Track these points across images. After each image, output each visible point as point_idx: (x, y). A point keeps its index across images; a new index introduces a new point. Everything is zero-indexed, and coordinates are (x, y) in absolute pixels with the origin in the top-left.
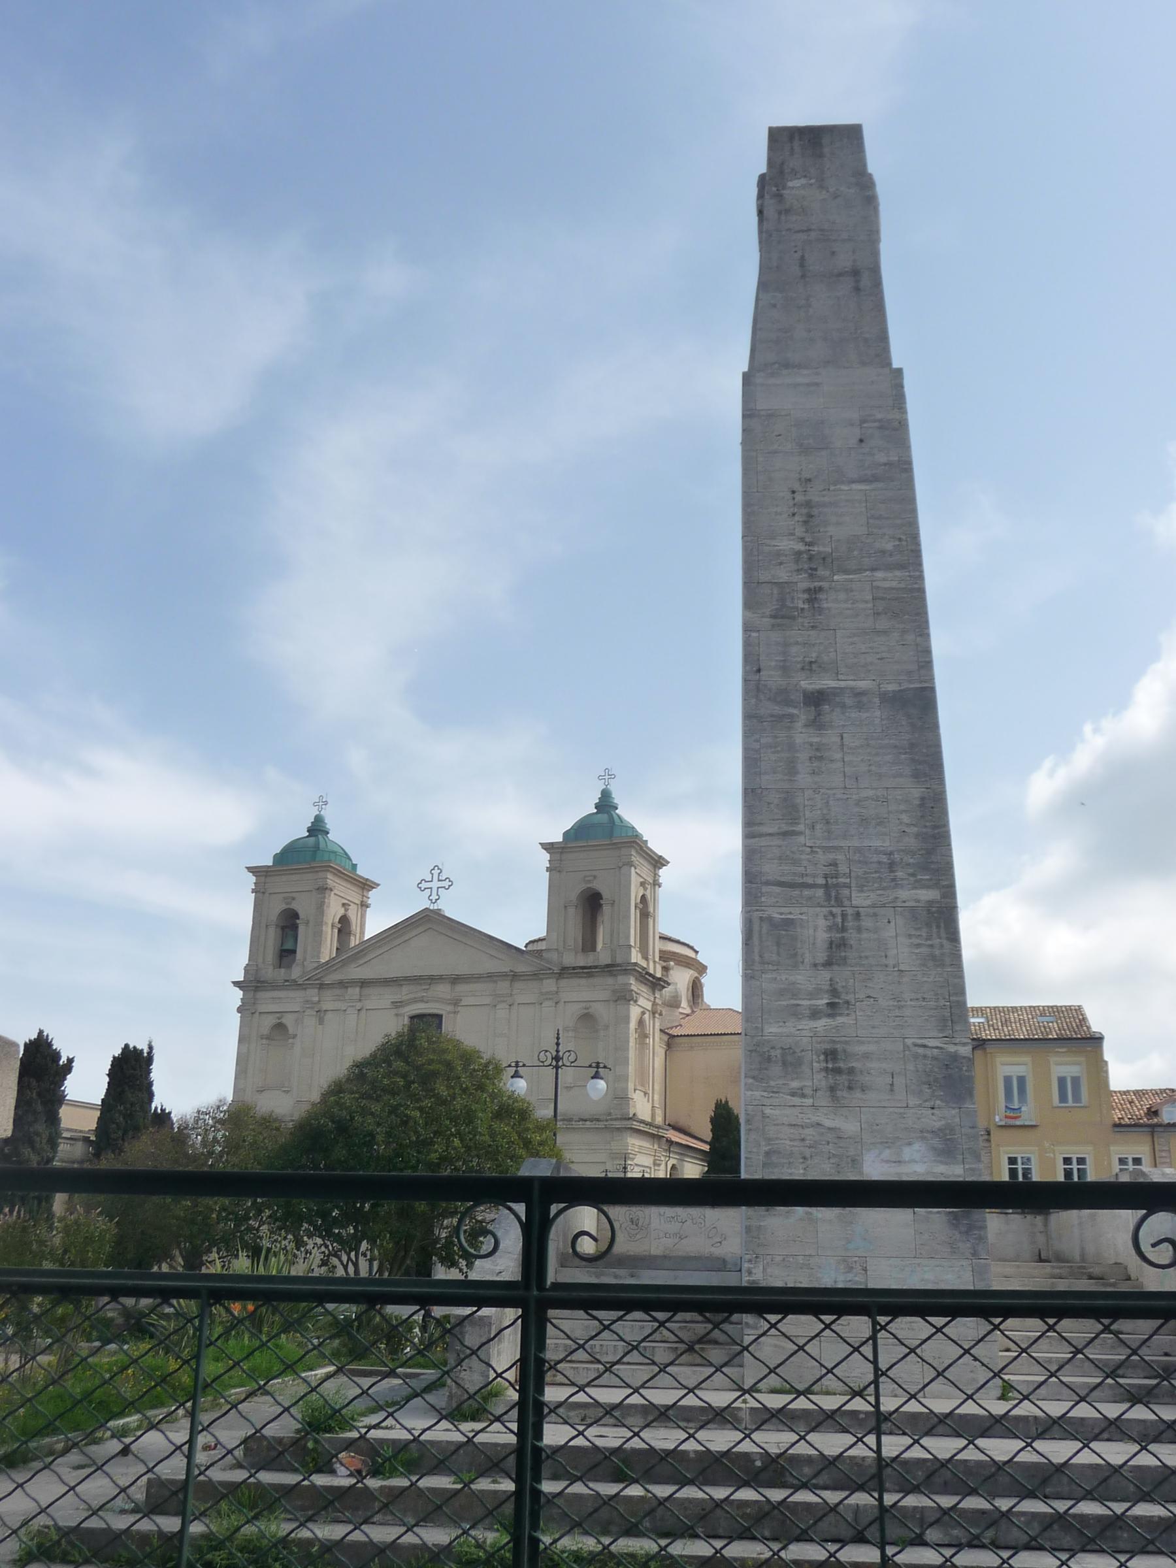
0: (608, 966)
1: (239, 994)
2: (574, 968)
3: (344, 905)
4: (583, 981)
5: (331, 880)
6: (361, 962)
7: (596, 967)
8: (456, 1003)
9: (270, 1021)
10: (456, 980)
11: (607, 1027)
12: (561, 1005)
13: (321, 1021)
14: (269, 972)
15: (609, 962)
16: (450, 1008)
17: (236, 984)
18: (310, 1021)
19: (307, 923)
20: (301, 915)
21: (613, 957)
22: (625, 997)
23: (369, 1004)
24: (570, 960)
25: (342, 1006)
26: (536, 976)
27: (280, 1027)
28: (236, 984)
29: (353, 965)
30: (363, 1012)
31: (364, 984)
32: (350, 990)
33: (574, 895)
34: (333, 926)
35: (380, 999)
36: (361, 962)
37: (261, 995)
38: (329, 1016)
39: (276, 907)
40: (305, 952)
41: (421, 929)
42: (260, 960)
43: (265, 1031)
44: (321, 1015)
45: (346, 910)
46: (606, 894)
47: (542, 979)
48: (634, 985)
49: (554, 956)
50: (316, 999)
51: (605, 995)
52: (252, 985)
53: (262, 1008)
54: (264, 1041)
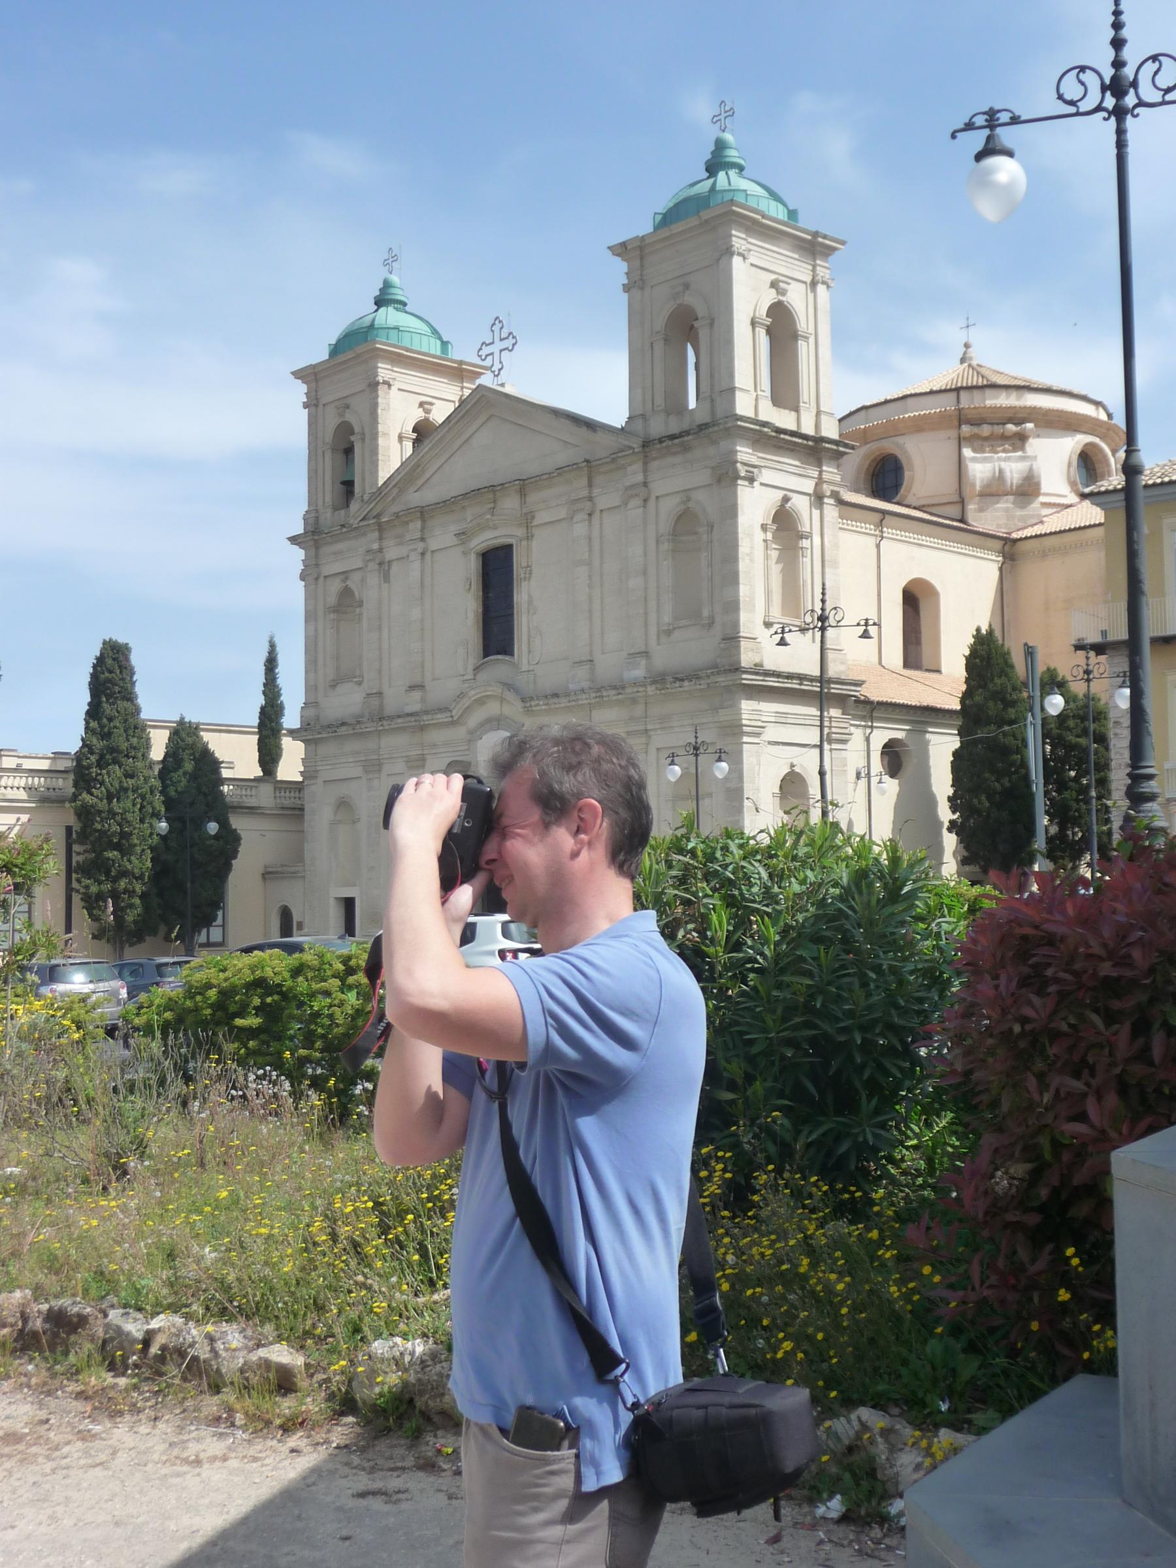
0: (702, 427)
1: (299, 554)
2: (661, 441)
3: (421, 405)
4: (678, 459)
5: (384, 371)
6: (420, 482)
7: (687, 433)
8: (527, 520)
9: (335, 586)
10: (523, 486)
11: (711, 526)
12: (652, 503)
13: (387, 578)
14: (327, 516)
15: (707, 419)
16: (520, 532)
17: (293, 540)
18: (373, 580)
19: (363, 440)
20: (357, 430)
21: (713, 411)
22: (727, 476)
23: (433, 544)
24: (657, 427)
25: (403, 551)
26: (615, 460)
27: (346, 593)
28: (293, 540)
29: (411, 490)
30: (428, 555)
31: (424, 513)
32: (411, 526)
33: (660, 322)
34: (401, 438)
35: (443, 535)
36: (420, 482)
37: (326, 550)
38: (395, 568)
39: (331, 422)
40: (363, 479)
41: (483, 418)
42: (320, 502)
43: (332, 600)
44: (384, 568)
45: (427, 412)
46: (701, 311)
47: (623, 467)
48: (745, 453)
49: (639, 425)
50: (376, 546)
51: (703, 477)
52: (313, 537)
53: (328, 569)
54: (332, 616)
